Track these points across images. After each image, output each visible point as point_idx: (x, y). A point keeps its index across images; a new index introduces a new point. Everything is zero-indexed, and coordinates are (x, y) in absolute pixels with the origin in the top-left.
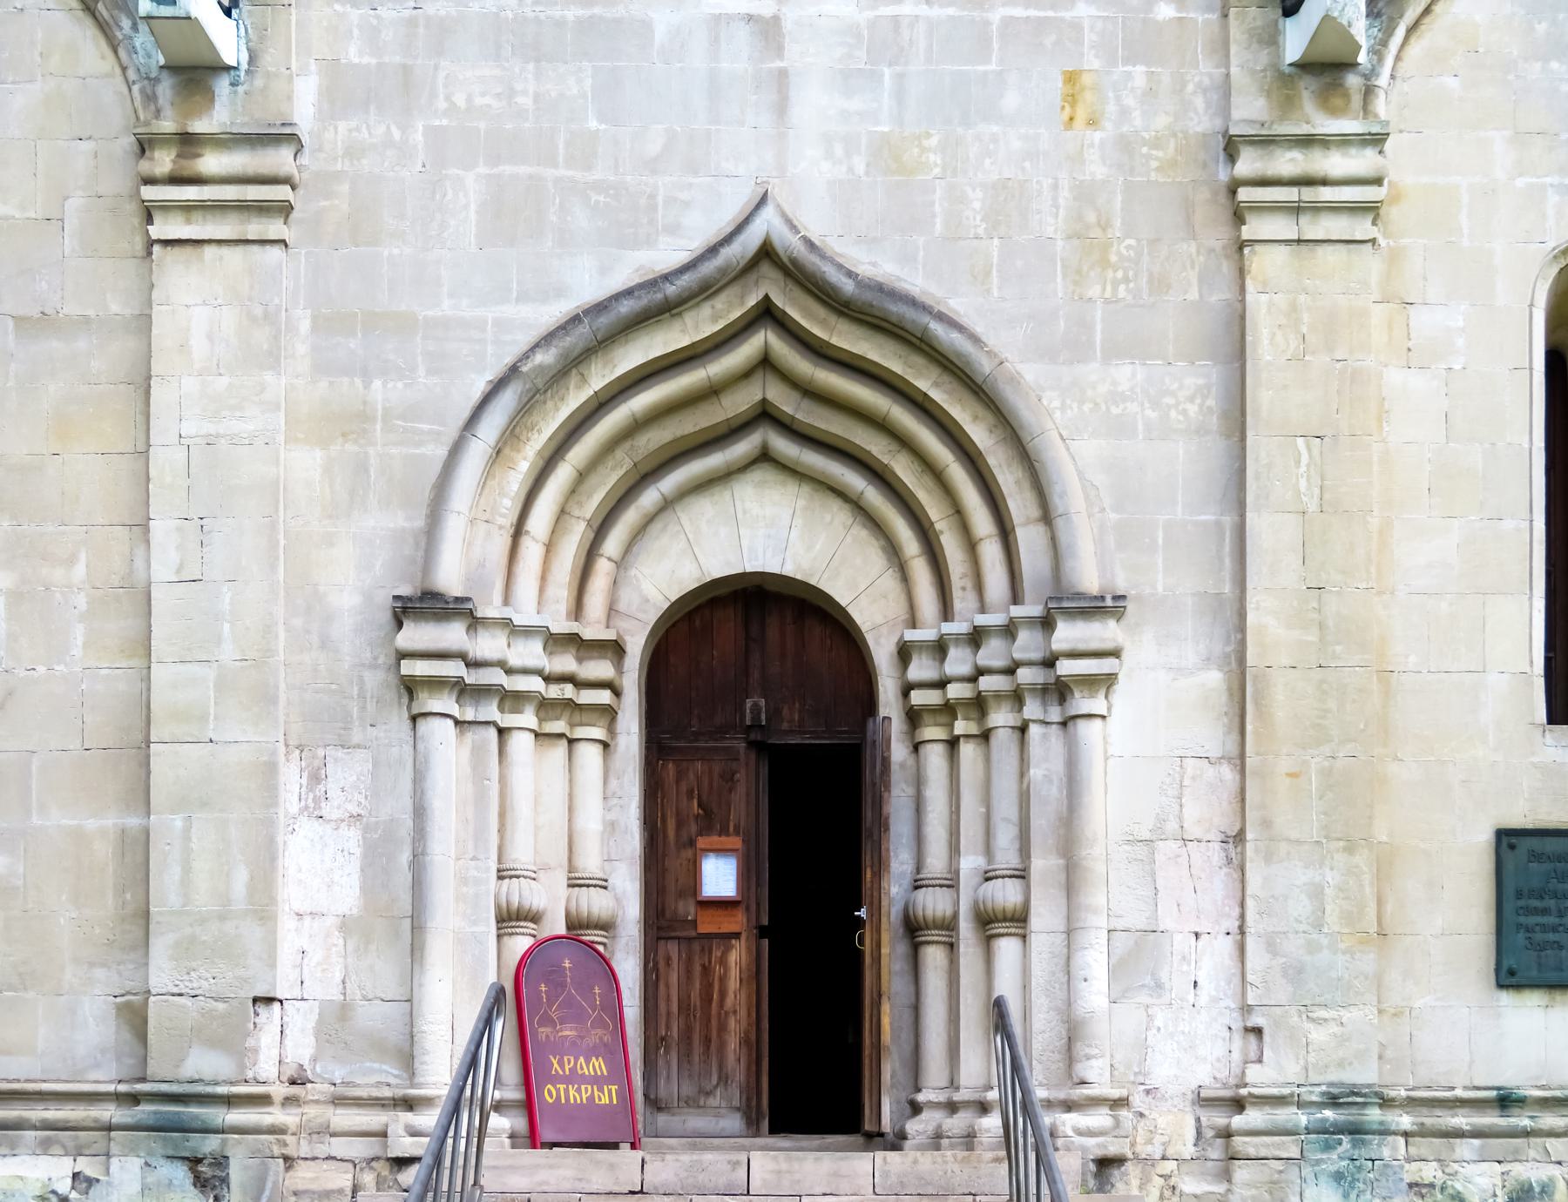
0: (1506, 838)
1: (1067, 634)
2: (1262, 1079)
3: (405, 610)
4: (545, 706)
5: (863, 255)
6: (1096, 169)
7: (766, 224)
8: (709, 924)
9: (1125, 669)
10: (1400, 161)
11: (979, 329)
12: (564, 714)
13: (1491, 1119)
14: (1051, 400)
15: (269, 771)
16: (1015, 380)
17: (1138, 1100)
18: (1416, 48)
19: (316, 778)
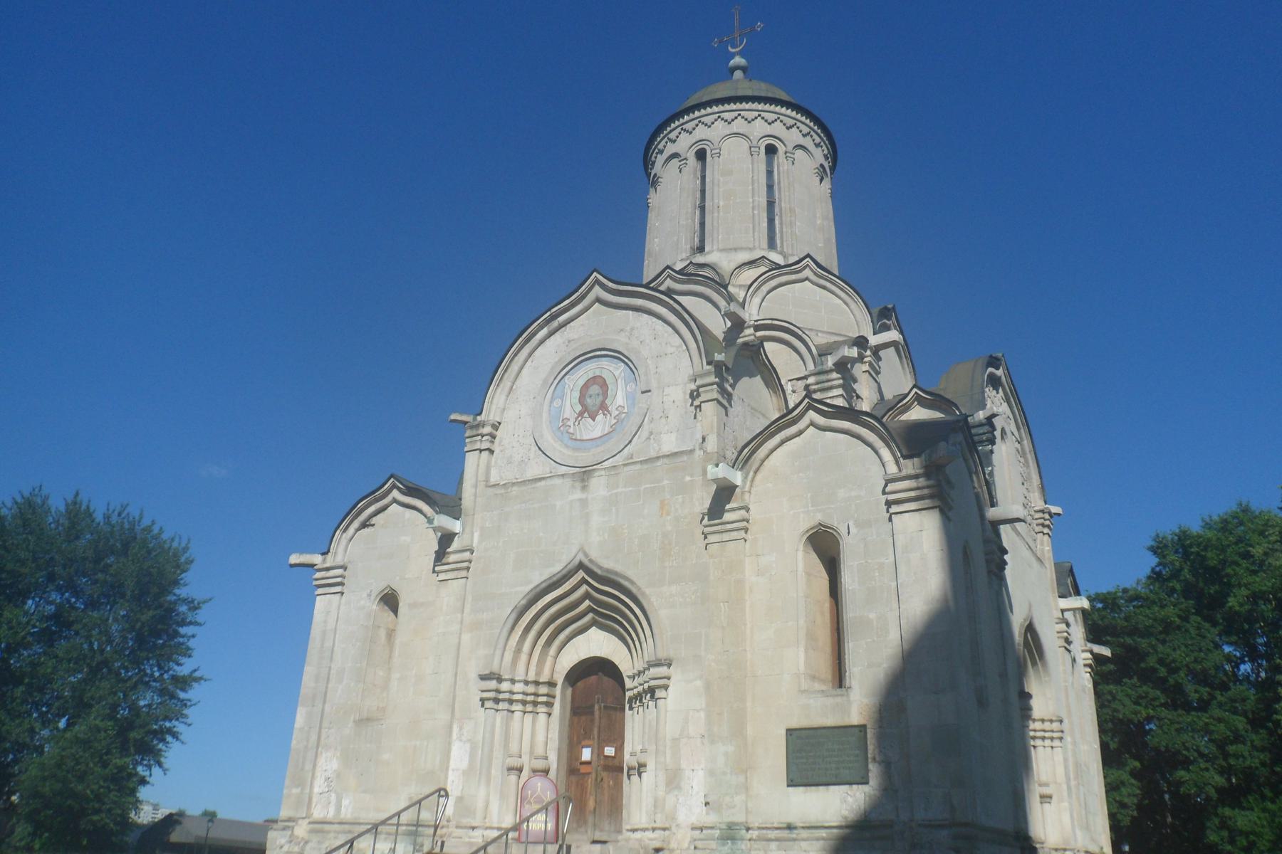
0: (790, 732)
1: (654, 671)
2: (711, 819)
3: (483, 678)
4: (524, 703)
5: (607, 562)
6: (669, 528)
7: (581, 557)
8: (583, 769)
9: (672, 683)
10: (755, 513)
11: (635, 579)
12: (531, 704)
13: (785, 834)
14: (653, 599)
15: (451, 727)
16: (643, 594)
17: (674, 829)
18: (759, 476)
19: (461, 728)
